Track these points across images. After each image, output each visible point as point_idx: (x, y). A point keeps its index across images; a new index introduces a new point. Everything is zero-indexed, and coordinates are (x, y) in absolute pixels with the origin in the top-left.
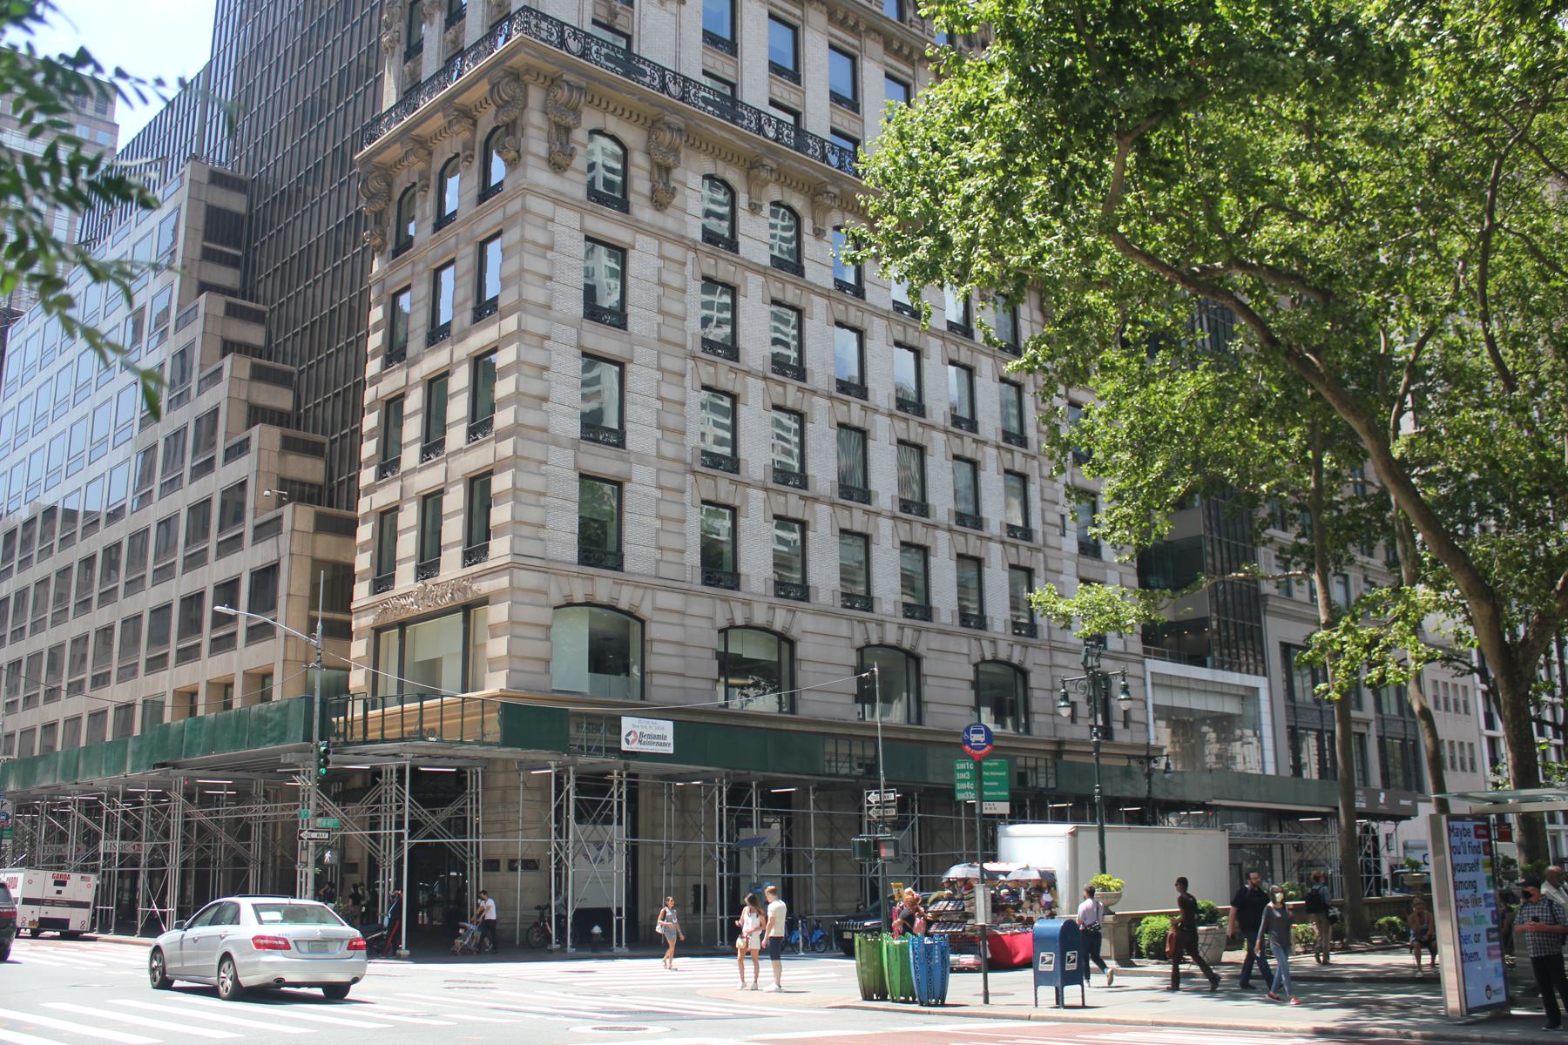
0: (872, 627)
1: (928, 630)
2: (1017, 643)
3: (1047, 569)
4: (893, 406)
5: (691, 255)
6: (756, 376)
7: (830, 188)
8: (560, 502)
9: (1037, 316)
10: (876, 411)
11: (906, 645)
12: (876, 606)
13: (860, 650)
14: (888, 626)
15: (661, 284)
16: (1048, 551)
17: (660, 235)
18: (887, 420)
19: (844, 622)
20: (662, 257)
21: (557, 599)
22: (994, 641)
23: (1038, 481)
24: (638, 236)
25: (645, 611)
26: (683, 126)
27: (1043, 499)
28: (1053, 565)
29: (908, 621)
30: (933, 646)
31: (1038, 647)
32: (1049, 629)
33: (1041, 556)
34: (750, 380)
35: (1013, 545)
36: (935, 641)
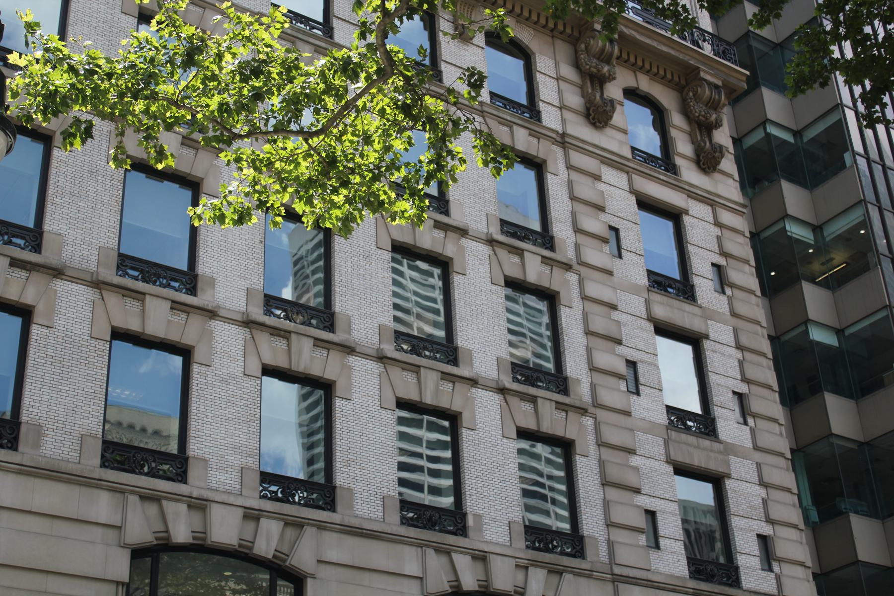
1: (321, 526)
2: (536, 564)
3: (601, 444)
9: (567, 71)
11: (265, 548)
12: (193, 473)
13: (138, 553)
14: (216, 513)
16: (601, 414)
22: (481, 557)
23: (577, 303)
27: (588, 333)
28: (612, 436)
29: (268, 505)
30: (333, 555)
31: (588, 574)
32: (611, 544)
33: (588, 422)
35: (524, 397)
36: (339, 548)
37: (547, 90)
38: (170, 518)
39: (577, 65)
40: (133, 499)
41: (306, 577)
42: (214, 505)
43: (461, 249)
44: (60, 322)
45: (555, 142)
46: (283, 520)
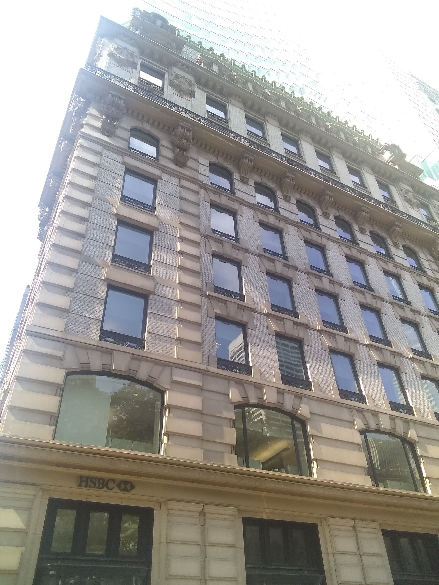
0: (369, 416)
4: (351, 284)
5: (202, 191)
6: (253, 254)
7: (288, 174)
8: (87, 298)
9: (430, 258)
10: (341, 285)
14: (381, 417)
15: (182, 198)
17: (179, 176)
18: (350, 292)
19: (345, 411)
20: (182, 187)
21: (74, 366)
24: (164, 174)
25: (163, 382)
26: (191, 129)
34: (249, 256)
37: (426, 264)
38: (367, 418)
39: (432, 255)
40: (354, 411)
41: (415, 443)
42: (380, 414)
43: (420, 318)
44: (312, 344)
45: (435, 282)
46: (402, 420)
